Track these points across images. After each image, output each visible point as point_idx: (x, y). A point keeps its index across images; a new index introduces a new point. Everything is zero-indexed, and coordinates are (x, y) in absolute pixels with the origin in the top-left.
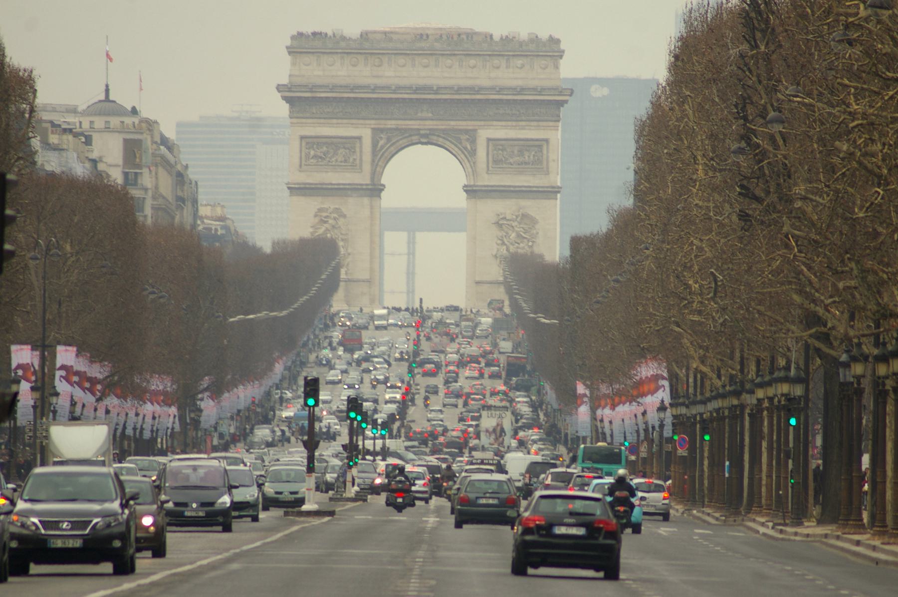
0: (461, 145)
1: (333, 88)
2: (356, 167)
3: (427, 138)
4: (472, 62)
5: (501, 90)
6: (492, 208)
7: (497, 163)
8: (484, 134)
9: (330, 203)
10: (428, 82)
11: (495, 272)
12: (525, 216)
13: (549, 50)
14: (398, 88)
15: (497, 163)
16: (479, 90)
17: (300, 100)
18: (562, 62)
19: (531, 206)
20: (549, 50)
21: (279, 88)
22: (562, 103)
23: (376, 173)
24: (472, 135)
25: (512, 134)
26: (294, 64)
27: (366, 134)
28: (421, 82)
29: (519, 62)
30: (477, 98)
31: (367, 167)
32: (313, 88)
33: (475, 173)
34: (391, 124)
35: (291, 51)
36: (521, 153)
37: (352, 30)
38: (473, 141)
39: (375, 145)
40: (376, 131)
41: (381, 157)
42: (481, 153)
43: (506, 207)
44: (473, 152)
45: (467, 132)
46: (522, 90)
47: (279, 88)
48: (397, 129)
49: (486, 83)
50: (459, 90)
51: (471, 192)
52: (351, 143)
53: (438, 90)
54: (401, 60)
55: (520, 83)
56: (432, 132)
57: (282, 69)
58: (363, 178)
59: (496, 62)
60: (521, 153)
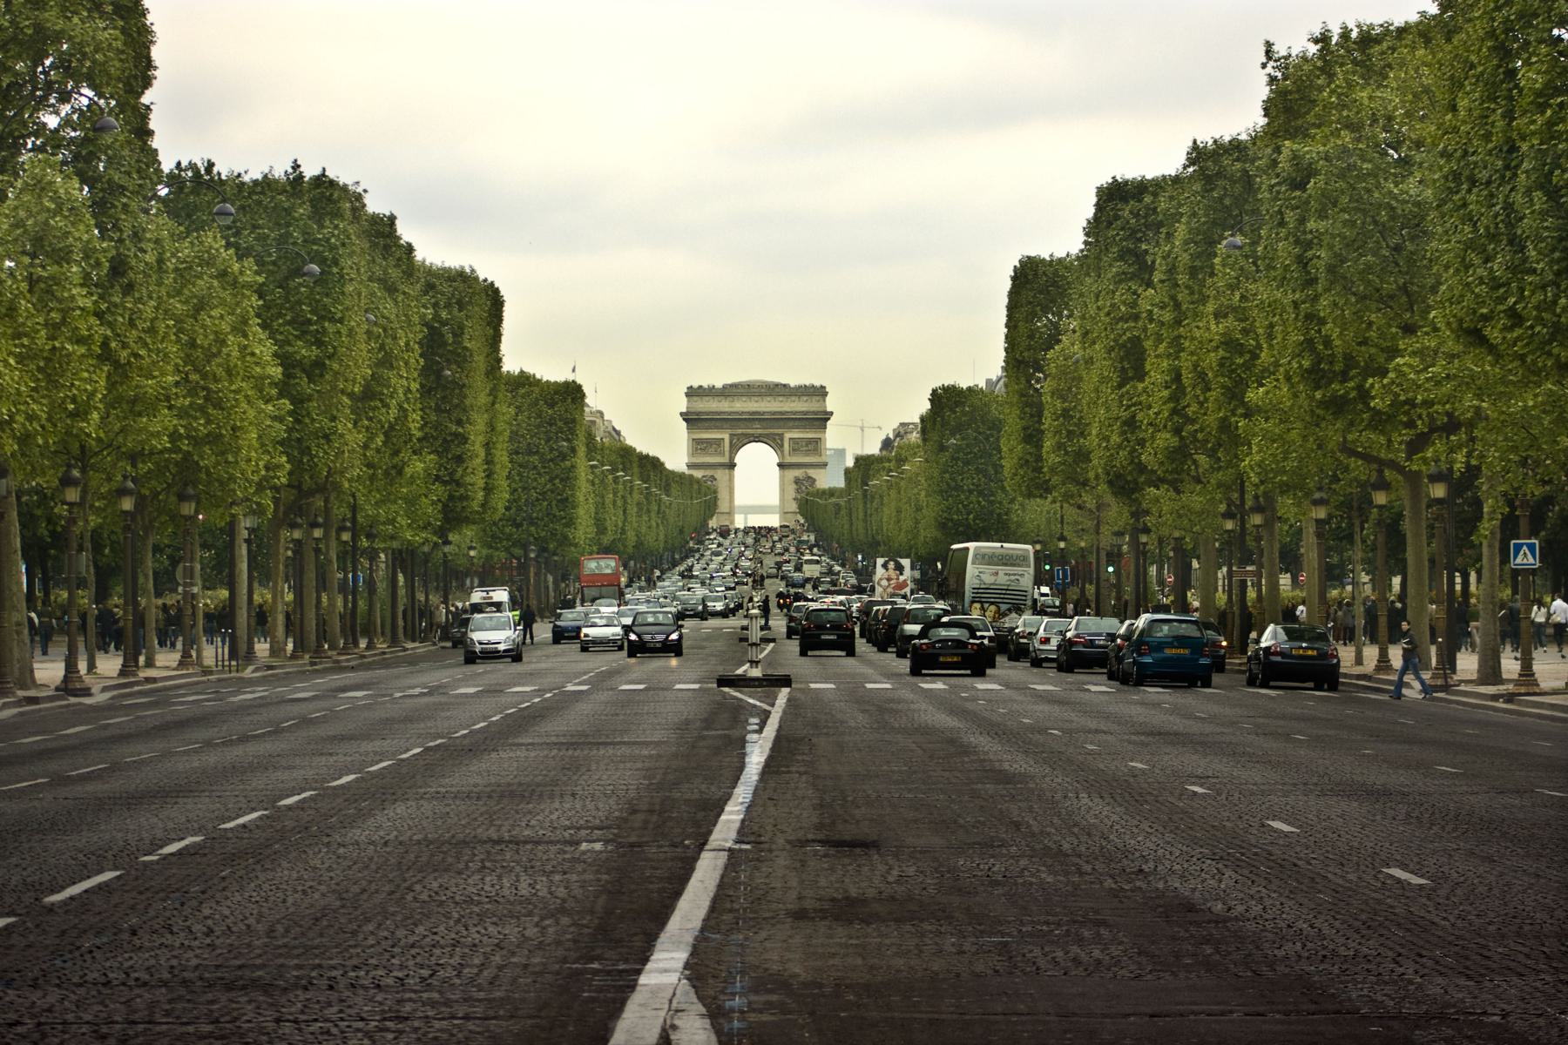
0: (775, 442)
3: (757, 439)
6: (792, 474)
7: (794, 450)
8: (787, 436)
9: (709, 473)
11: (794, 507)
13: (821, 392)
15: (794, 450)
17: (691, 419)
18: (828, 399)
20: (821, 392)
23: (732, 458)
24: (781, 436)
27: (726, 437)
35: (687, 395)
37: (719, 385)
41: (735, 448)
43: (798, 473)
44: (782, 446)
46: (806, 413)
51: (780, 465)
52: (719, 442)
58: (726, 460)
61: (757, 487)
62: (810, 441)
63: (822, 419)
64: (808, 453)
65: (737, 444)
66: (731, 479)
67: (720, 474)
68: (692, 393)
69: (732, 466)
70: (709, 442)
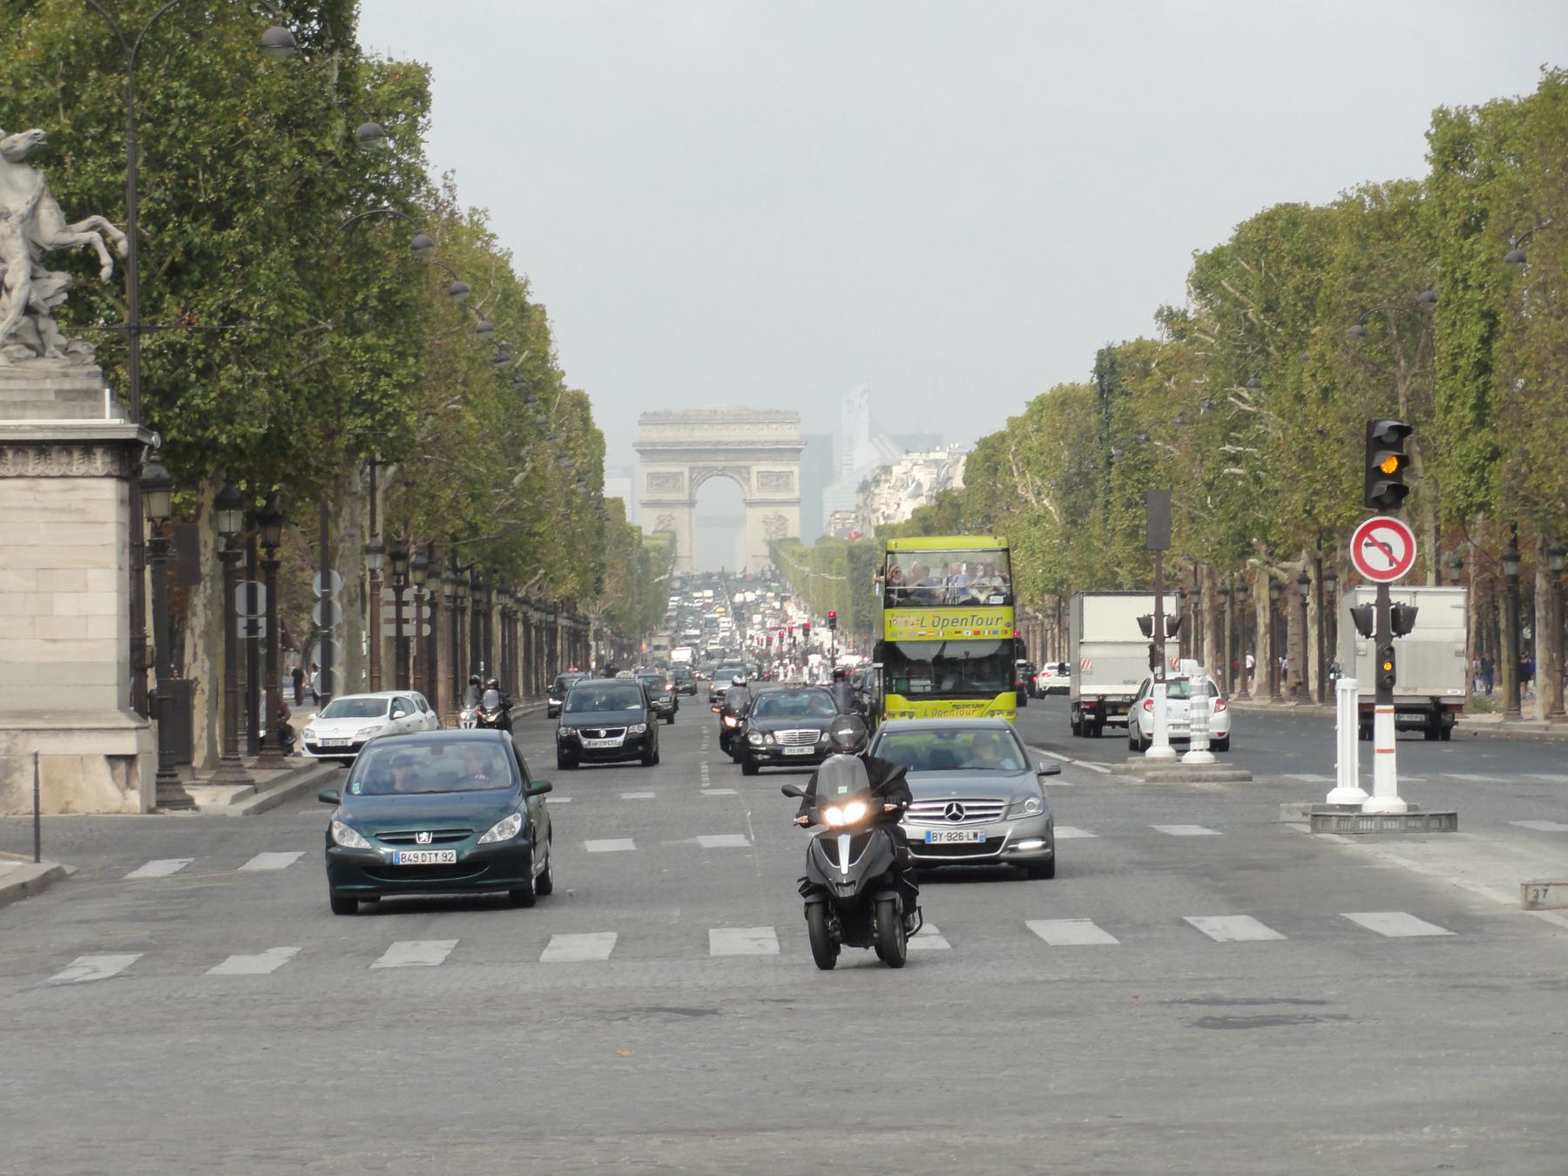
1: (666, 444)
3: (722, 472)
9: (666, 512)
12: (780, 517)
19: (783, 510)
24: (747, 468)
27: (686, 470)
31: (687, 491)
34: (701, 464)
40: (692, 469)
41: (694, 484)
43: (769, 511)
48: (704, 468)
50: (740, 443)
52: (676, 476)
58: (683, 496)
62: (780, 475)
69: (691, 504)
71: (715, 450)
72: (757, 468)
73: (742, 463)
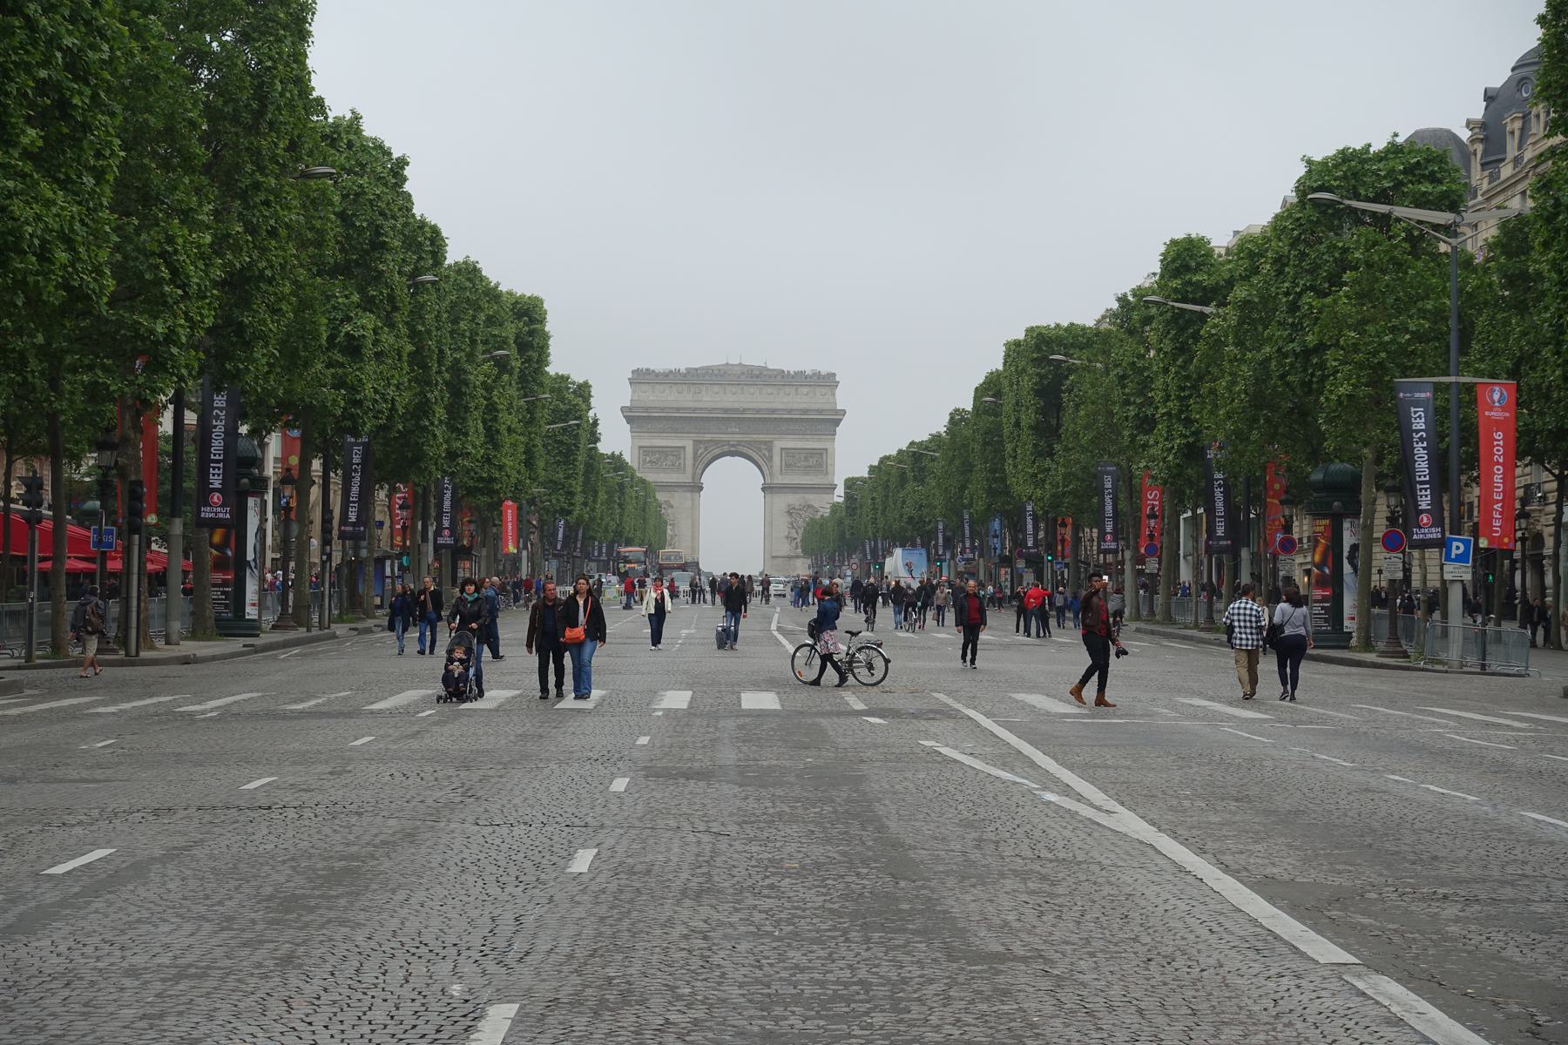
1: (662, 409)
2: (681, 469)
4: (770, 390)
5: (790, 411)
7: (788, 467)
8: (779, 444)
10: (736, 406)
11: (785, 548)
13: (828, 381)
14: (711, 410)
15: (788, 467)
16: (773, 411)
18: (838, 391)
20: (828, 381)
21: (623, 409)
22: (837, 422)
24: (769, 445)
25: (799, 445)
26: (634, 392)
27: (689, 445)
28: (729, 406)
29: (805, 390)
30: (769, 415)
31: (689, 470)
32: (647, 409)
33: (771, 474)
34: (708, 437)
36: (806, 459)
38: (770, 451)
39: (695, 454)
40: (697, 443)
42: (776, 459)
43: (794, 499)
44: (771, 458)
45: (765, 443)
46: (806, 411)
47: (623, 409)
49: (781, 406)
53: (744, 411)
54: (716, 389)
55: (802, 406)
56: (739, 443)
57: (625, 396)
58: (686, 478)
59: (787, 390)
60: (806, 459)
61: (732, 520)
63: (830, 422)
64: (807, 470)
65: (708, 455)
66: (695, 508)
67: (679, 499)
68: (641, 378)
70: (664, 452)
71: (730, 418)
72: (779, 444)
73: (762, 437)
